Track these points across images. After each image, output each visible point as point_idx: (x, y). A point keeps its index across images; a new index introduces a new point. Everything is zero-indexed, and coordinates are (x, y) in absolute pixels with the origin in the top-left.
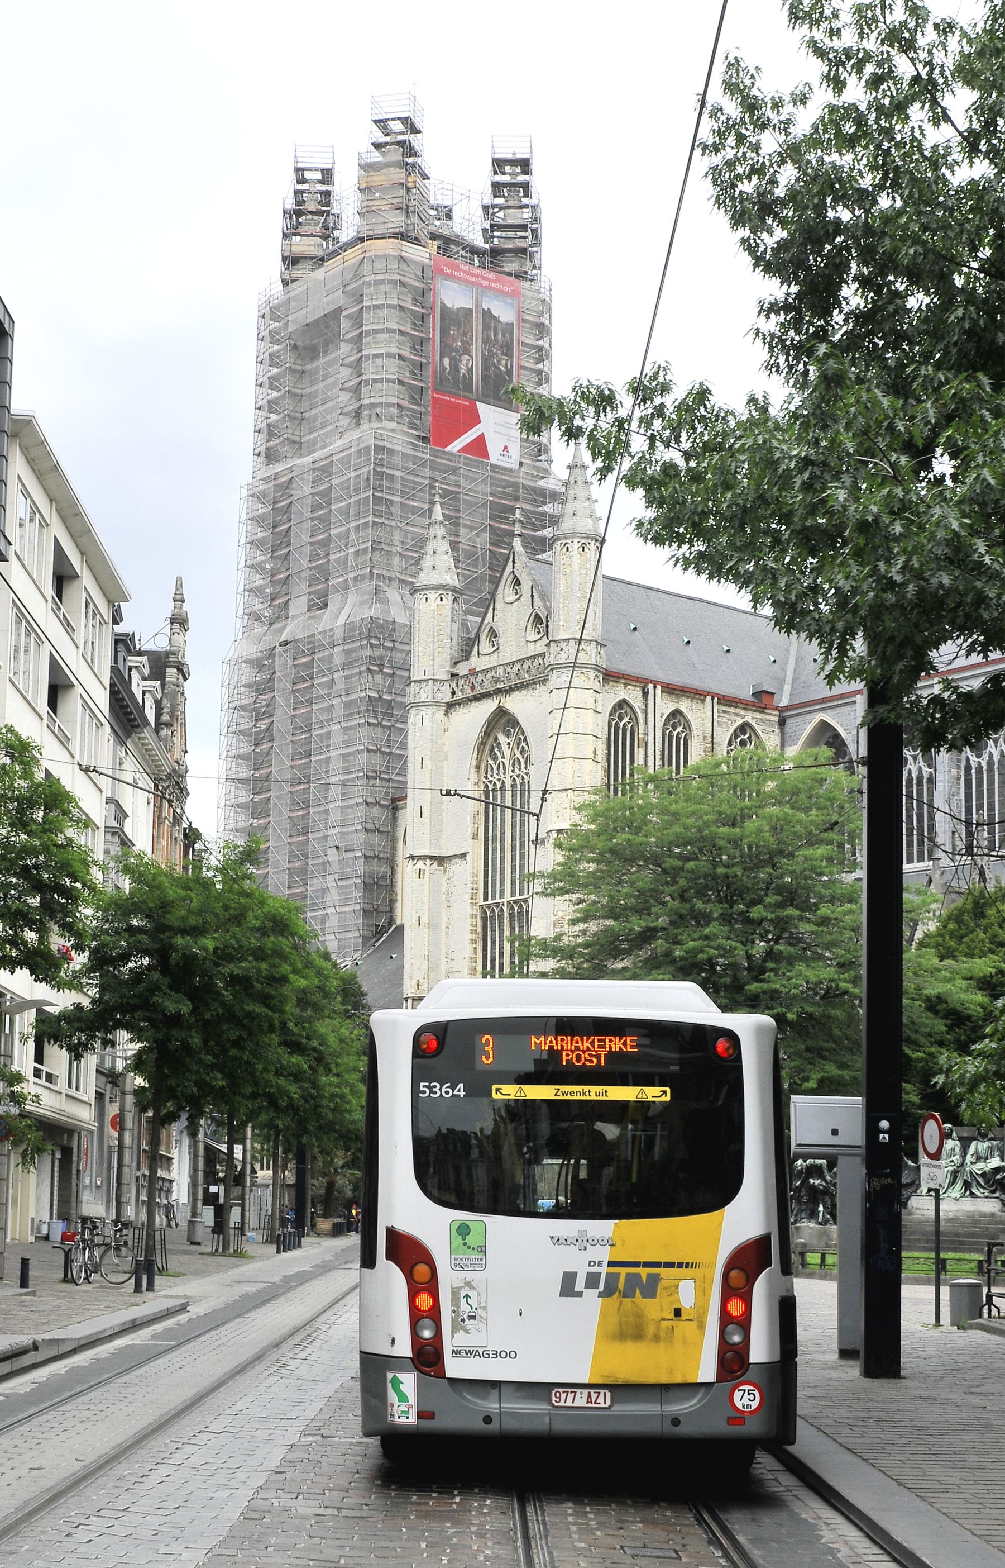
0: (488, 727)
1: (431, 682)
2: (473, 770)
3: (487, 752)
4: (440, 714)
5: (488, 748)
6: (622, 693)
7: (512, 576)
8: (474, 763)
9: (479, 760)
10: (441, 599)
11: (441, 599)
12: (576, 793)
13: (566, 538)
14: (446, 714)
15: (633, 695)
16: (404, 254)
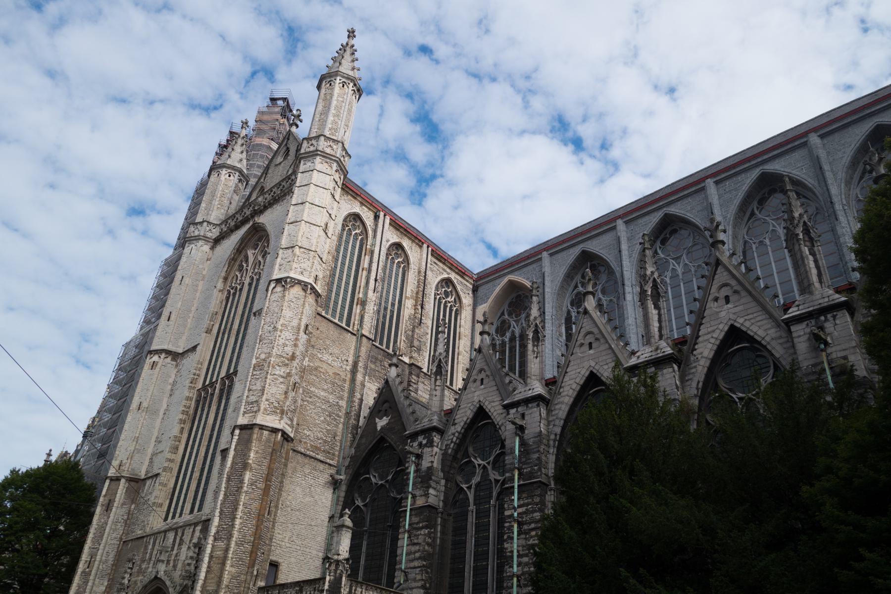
0: (241, 244)
1: (205, 224)
2: (221, 280)
3: (236, 267)
4: (206, 248)
5: (238, 263)
6: (358, 209)
7: (285, 148)
8: (223, 274)
9: (228, 273)
10: (230, 176)
11: (230, 176)
12: (302, 250)
13: (331, 77)
14: (212, 248)
15: (367, 216)
16: (271, 146)
